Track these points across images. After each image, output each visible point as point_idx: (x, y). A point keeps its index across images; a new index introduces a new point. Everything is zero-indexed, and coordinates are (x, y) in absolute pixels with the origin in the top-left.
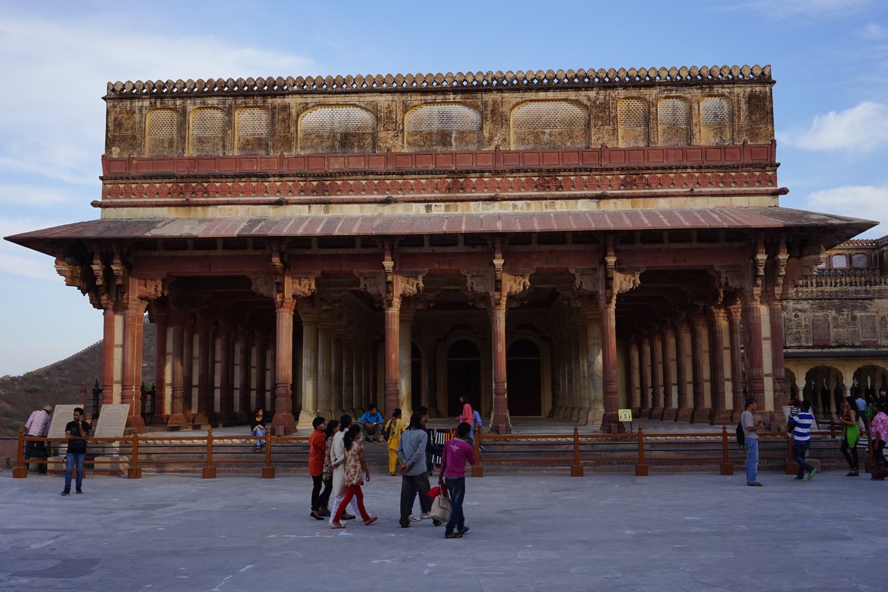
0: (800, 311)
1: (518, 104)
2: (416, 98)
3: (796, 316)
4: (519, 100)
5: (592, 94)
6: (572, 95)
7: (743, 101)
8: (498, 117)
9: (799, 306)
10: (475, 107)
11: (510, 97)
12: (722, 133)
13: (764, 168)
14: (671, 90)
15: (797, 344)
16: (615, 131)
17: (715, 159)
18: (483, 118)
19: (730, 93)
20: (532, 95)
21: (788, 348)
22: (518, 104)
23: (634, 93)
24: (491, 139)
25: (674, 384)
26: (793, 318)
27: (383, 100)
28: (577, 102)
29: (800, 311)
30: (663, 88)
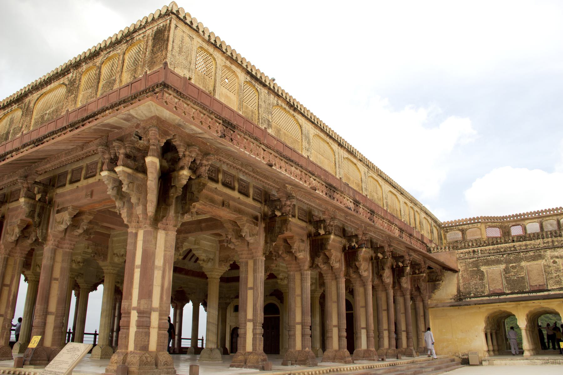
0: (557, 257)
3: (554, 262)
4: (39, 96)
5: (70, 75)
6: (62, 81)
7: (151, 38)
8: (28, 112)
9: (556, 254)
10: (21, 108)
11: (36, 95)
12: (135, 72)
13: (153, 90)
14: (110, 52)
15: (558, 286)
16: (76, 97)
17: (125, 94)
18: (22, 115)
19: (143, 37)
20: (44, 90)
21: (549, 290)
24: (22, 128)
25: (363, 328)
26: (551, 264)
29: (557, 257)
30: (105, 52)
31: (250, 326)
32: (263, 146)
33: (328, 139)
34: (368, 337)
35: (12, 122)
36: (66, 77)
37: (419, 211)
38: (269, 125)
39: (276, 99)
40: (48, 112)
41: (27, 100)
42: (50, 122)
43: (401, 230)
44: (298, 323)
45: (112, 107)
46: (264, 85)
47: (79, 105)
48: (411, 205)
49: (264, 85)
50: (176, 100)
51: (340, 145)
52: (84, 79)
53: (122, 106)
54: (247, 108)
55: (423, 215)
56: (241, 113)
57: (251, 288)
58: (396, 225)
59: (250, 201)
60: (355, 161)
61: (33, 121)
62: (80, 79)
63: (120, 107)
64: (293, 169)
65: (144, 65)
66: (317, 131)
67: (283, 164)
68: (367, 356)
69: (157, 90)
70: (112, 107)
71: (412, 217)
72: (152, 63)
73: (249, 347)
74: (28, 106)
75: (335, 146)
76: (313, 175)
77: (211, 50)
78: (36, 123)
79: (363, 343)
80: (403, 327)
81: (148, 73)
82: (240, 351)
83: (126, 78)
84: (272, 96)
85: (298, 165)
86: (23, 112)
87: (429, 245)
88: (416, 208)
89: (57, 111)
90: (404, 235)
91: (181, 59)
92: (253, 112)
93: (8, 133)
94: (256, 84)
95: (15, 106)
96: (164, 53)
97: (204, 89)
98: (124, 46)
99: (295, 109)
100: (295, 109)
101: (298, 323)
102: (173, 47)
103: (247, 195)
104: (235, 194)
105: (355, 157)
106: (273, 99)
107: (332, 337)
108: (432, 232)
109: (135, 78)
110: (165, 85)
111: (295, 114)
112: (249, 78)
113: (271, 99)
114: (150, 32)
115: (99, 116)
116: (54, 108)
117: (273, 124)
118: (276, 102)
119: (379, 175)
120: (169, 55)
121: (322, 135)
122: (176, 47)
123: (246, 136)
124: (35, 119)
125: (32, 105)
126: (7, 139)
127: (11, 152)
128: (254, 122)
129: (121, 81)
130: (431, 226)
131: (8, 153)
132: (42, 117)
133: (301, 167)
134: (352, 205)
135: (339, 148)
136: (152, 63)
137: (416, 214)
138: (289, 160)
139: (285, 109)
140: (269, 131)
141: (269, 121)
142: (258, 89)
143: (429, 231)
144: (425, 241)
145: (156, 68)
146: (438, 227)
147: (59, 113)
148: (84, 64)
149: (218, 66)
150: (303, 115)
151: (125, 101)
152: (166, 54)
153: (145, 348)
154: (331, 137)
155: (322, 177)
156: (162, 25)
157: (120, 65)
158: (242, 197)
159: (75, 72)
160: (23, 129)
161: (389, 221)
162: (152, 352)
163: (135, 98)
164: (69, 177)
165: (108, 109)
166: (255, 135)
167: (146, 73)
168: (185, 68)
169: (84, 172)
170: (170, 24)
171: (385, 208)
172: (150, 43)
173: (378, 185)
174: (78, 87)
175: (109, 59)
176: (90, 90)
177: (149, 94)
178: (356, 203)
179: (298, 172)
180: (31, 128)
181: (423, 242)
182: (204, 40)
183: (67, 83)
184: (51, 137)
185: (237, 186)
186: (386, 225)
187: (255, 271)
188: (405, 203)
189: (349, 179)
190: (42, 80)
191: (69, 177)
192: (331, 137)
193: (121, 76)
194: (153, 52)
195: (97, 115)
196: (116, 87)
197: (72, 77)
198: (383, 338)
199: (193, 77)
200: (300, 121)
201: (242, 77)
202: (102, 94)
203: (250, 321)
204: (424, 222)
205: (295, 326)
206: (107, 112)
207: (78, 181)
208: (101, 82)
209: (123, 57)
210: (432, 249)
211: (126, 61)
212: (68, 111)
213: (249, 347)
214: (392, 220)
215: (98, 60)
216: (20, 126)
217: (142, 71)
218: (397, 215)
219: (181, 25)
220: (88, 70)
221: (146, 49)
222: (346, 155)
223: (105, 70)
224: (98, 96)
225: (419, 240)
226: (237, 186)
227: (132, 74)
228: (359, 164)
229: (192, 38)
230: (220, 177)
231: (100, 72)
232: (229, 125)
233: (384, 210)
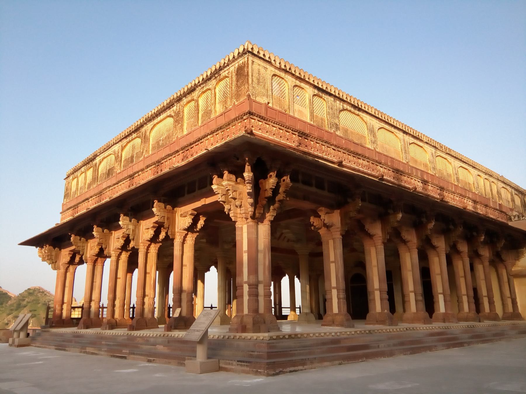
1: (152, 129)
2: (125, 141)
5: (175, 108)
6: (168, 112)
7: (234, 74)
8: (145, 139)
10: (139, 137)
11: (150, 125)
12: (226, 103)
13: (242, 118)
14: (203, 87)
16: (182, 126)
17: (222, 121)
18: (142, 142)
19: (228, 73)
20: (156, 121)
22: (152, 129)
23: (189, 98)
24: (143, 152)
25: (440, 294)
27: (116, 148)
28: (170, 116)
30: (200, 88)
31: (334, 292)
32: (333, 147)
33: (392, 129)
34: (445, 301)
35: (134, 147)
36: (172, 109)
37: (495, 181)
38: (337, 128)
39: (341, 104)
40: (161, 139)
41: (143, 130)
42: (164, 146)
43: (475, 202)
44: (376, 290)
45: (212, 133)
46: (330, 95)
47: (185, 132)
48: (487, 177)
49: (330, 95)
50: (261, 123)
51: (405, 132)
52: (186, 110)
53: (219, 131)
54: (317, 116)
55: (501, 185)
56: (312, 123)
57: (332, 262)
58: (469, 198)
59: (325, 193)
60: (421, 144)
61: (151, 146)
62: (183, 111)
63: (218, 132)
64: (361, 161)
65: (232, 97)
66: (382, 124)
67: (351, 158)
68: (445, 318)
69: (245, 117)
70: (212, 133)
71: (488, 188)
72: (238, 96)
73: (335, 310)
74: (145, 135)
75: (401, 135)
76: (380, 163)
77: (282, 74)
78: (153, 148)
79: (441, 306)
80: (484, 292)
81: (236, 103)
82: (328, 312)
83: (219, 109)
84: (338, 102)
85: (365, 157)
86: (142, 140)
87: (510, 213)
88: (491, 179)
89: (168, 137)
90: (478, 207)
91: (259, 89)
92: (322, 119)
93: (132, 157)
94: (323, 95)
95: (134, 135)
96: (246, 87)
97: (281, 109)
98: (213, 82)
99: (360, 110)
100: (360, 110)
101: (376, 290)
102: (252, 81)
103: (322, 188)
104: (313, 189)
105: (421, 141)
106: (339, 104)
107: (409, 301)
108: (513, 200)
109: (226, 108)
110: (250, 113)
111: (360, 113)
112: (316, 92)
113: (338, 105)
114: (233, 68)
115: (203, 140)
116: (166, 135)
117: (341, 126)
118: (341, 107)
119: (447, 153)
120: (250, 88)
121: (387, 127)
122: (255, 79)
123: (318, 142)
124: (152, 145)
125: (148, 133)
126: (132, 161)
127: (138, 172)
128: (324, 128)
129: (216, 111)
130: (512, 195)
131: (135, 173)
132: (158, 143)
133: (368, 158)
134: (420, 184)
135: (405, 135)
136: (238, 96)
137: (492, 183)
138: (356, 154)
139: (350, 111)
140: (338, 133)
141: (336, 124)
142: (325, 99)
143: (510, 200)
144: (504, 210)
145: (242, 100)
146: (520, 195)
147: (171, 139)
148: (184, 98)
149: (290, 87)
150: (367, 113)
151: (221, 128)
152: (248, 88)
153: (256, 311)
154: (395, 127)
155: (389, 164)
156: (241, 62)
157: (213, 98)
158: (319, 192)
159: (178, 105)
160: (144, 154)
161: (461, 195)
162: (261, 314)
163: (229, 124)
164: (186, 189)
165: (209, 134)
166: (325, 139)
167: (234, 104)
168: (264, 95)
169: (197, 185)
170: (248, 61)
171: (456, 184)
172: (234, 79)
173: (447, 164)
174: (183, 117)
175: (204, 92)
176: (193, 120)
177: (239, 121)
178: (425, 182)
179: (367, 163)
180: (150, 153)
181: (502, 212)
182: (276, 68)
183: (173, 114)
184: (168, 159)
185: (314, 182)
186: (458, 199)
187: (335, 248)
188: (478, 175)
189: (416, 161)
190: (153, 113)
191: (186, 189)
192: (395, 127)
193: (215, 107)
194: (238, 86)
195: (201, 139)
196: (213, 116)
197: (177, 109)
198: (462, 302)
199: (271, 101)
200: (365, 119)
201: (310, 91)
202: (202, 123)
203: (334, 288)
204: (503, 191)
205: (374, 292)
206: (209, 137)
207: (194, 191)
208: (200, 112)
209: (215, 91)
210: (513, 217)
211: (217, 94)
212: (177, 137)
213: (335, 310)
214: (463, 194)
215: (195, 94)
216: (142, 151)
217: (231, 102)
218: (470, 188)
219: (256, 60)
220: (189, 102)
221: (232, 83)
222: (412, 140)
223: (201, 102)
224: (200, 124)
225: (497, 210)
226: (314, 182)
227: (223, 105)
228: (426, 146)
229: (266, 68)
230: (300, 177)
231: (198, 104)
232: (303, 135)
233: (455, 185)
